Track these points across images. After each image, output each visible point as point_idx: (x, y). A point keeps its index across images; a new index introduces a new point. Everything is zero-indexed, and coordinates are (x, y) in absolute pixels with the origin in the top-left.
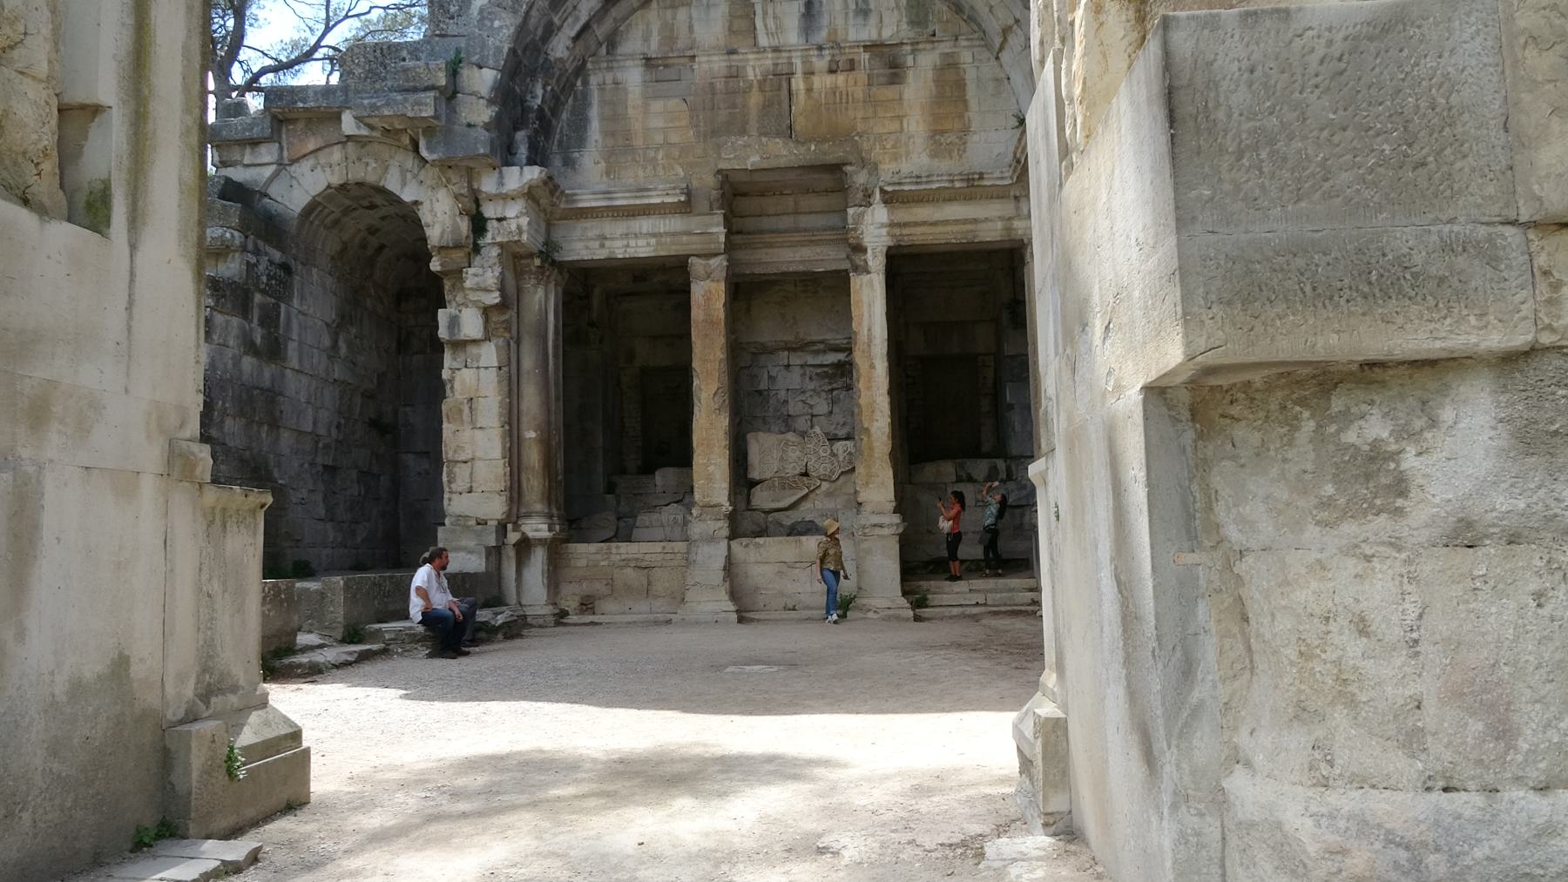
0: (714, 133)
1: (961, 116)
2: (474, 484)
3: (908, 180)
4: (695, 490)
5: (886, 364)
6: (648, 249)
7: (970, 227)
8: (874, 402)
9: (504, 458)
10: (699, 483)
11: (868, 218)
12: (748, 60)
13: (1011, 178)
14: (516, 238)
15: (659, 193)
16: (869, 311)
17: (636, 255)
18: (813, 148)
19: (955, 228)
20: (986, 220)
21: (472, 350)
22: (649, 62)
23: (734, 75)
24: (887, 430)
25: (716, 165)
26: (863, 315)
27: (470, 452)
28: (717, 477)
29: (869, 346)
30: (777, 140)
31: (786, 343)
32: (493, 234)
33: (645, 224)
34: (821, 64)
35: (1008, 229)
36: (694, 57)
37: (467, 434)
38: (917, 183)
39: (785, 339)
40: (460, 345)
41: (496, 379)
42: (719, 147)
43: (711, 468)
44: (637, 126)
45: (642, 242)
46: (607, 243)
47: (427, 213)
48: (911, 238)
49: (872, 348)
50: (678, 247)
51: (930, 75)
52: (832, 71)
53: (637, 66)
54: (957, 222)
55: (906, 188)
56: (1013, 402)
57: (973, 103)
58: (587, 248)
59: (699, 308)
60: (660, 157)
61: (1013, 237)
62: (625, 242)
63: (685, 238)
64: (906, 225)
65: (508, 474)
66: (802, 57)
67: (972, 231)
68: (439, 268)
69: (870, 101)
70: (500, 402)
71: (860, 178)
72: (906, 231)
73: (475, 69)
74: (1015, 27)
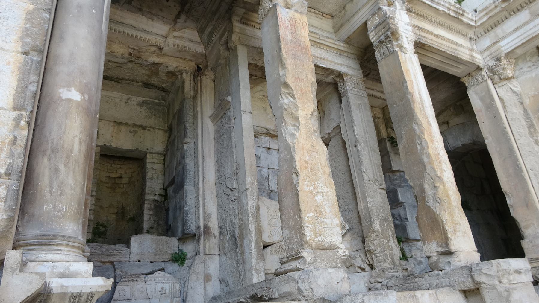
4: (306, 224)
8: (439, 154)
9: (15, 108)
10: (307, 216)
16: (416, 80)
19: (448, 44)
28: (328, 211)
29: (423, 106)
39: (268, 127)
43: (319, 198)
48: (426, 40)
49: (425, 108)
54: (448, 40)
56: (403, 201)
61: (474, 62)
64: (422, 29)
65: (22, 142)
67: (456, 50)
72: (423, 34)
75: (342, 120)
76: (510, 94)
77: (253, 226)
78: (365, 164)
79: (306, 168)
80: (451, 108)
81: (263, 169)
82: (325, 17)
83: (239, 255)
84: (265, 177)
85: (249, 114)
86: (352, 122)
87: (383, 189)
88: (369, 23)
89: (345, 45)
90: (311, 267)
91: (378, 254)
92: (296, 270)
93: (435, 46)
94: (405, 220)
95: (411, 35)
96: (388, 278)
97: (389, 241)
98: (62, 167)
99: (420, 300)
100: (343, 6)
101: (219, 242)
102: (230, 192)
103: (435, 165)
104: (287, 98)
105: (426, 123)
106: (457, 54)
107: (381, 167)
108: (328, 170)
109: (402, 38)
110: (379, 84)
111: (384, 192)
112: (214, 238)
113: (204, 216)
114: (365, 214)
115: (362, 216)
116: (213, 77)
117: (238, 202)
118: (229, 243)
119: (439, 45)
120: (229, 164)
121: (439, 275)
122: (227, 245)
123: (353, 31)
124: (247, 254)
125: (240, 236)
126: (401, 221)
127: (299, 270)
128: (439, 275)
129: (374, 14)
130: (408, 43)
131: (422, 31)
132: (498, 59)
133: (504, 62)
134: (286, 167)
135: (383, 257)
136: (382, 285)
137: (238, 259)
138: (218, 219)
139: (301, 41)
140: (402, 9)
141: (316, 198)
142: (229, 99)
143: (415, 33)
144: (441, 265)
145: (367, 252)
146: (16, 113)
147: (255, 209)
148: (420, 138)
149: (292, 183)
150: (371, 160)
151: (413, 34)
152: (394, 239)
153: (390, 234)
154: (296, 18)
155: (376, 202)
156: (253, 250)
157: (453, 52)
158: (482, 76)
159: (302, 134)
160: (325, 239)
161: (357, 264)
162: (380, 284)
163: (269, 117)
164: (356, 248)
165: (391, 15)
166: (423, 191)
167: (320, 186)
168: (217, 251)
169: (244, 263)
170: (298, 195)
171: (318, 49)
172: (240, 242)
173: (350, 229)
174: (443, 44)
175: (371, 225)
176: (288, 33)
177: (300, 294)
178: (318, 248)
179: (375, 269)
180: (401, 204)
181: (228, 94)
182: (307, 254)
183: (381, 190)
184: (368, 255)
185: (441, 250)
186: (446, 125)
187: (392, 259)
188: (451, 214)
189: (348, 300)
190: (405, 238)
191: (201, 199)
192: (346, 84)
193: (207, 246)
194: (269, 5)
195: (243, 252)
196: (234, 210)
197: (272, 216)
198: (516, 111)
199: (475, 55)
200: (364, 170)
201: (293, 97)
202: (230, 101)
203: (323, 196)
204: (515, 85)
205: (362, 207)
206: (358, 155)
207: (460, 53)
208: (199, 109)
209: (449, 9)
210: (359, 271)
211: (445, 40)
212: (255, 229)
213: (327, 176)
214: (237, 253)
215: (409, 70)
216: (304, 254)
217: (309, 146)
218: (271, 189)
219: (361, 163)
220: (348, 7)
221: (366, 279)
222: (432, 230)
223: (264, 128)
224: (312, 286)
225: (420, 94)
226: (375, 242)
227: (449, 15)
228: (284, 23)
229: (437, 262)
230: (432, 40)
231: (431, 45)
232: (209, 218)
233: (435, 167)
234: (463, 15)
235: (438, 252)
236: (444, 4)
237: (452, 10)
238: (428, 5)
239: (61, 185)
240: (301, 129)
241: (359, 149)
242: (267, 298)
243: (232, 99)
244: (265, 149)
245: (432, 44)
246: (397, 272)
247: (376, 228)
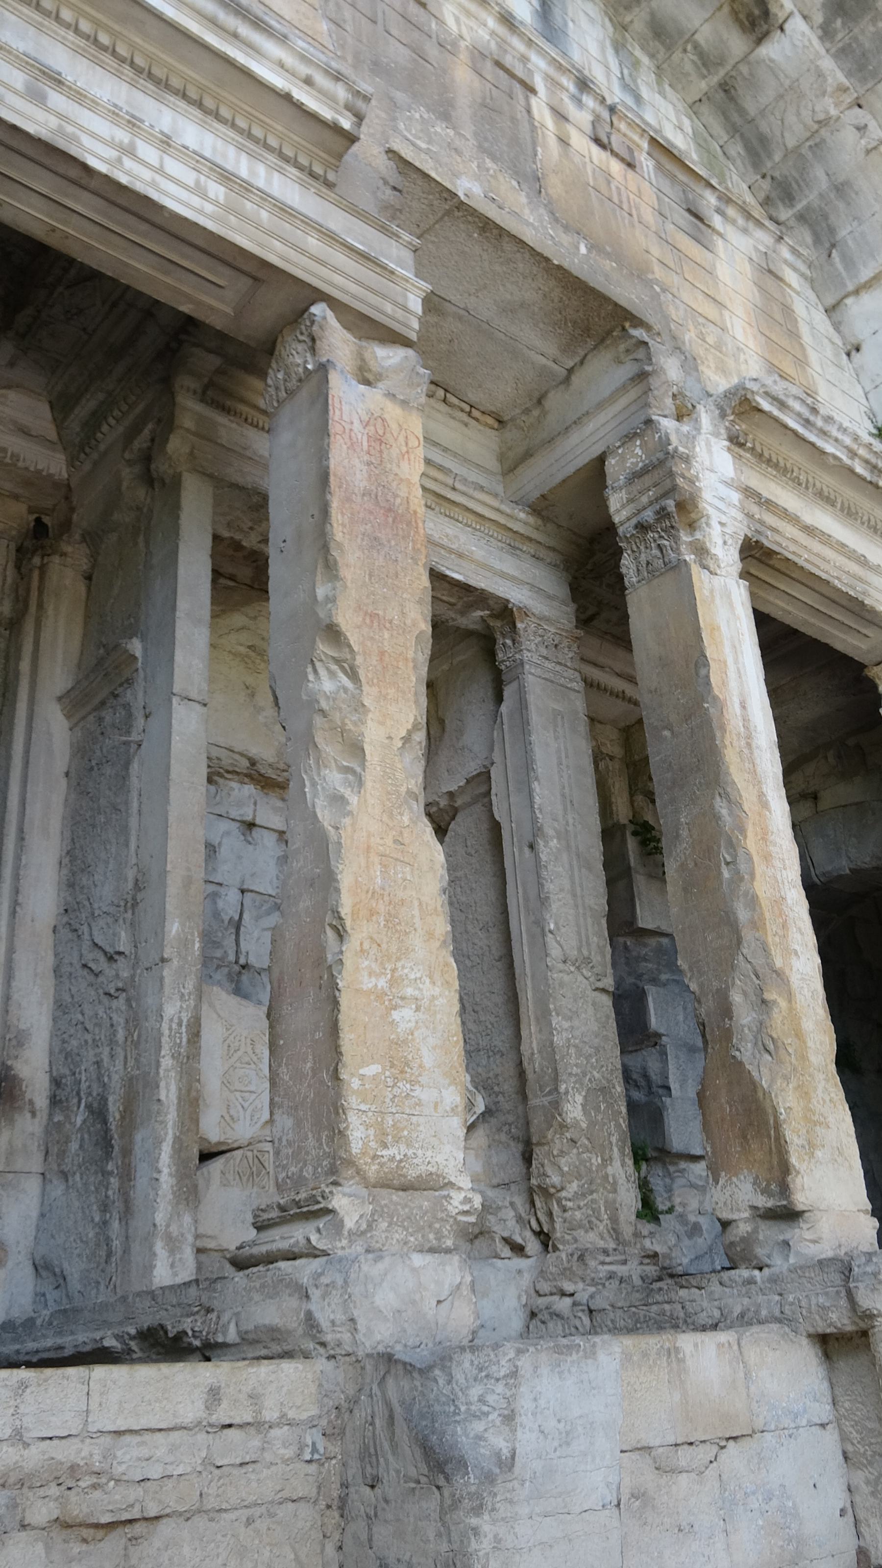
4: (352, 1102)
7: (854, 568)
16: (736, 661)
17: (154, 195)
18: (583, 250)
19: (841, 560)
26: (725, 662)
28: (428, 1058)
29: (749, 745)
31: (253, 763)
38: (807, 423)
39: (254, 751)
43: (404, 1016)
46: (56, 99)
48: (778, 538)
49: (756, 753)
52: (597, 141)
54: (841, 548)
56: (662, 1031)
59: (352, 446)
62: (122, 136)
63: (313, 243)
64: (768, 504)
67: (860, 580)
72: (771, 520)
75: (497, 756)
77: (173, 1088)
78: (554, 907)
79: (372, 913)
80: (831, 754)
81: (222, 891)
82: (477, 420)
83: (114, 1181)
84: (226, 918)
85: (198, 707)
86: (528, 765)
87: (603, 990)
88: (611, 462)
89: (531, 520)
90: (358, 1248)
91: (570, 1200)
92: (307, 1255)
93: (801, 562)
94: (661, 1091)
95: (735, 519)
96: (594, 1282)
97: (607, 1161)
99: (689, 1362)
100: (536, 395)
101: (47, 1132)
102: (102, 964)
103: (769, 933)
104: (332, 674)
105: (755, 799)
106: (864, 593)
107: (604, 922)
108: (442, 926)
109: (708, 524)
110: (621, 653)
111: (606, 1001)
112: (28, 1115)
114: (542, 1070)
115: (530, 1075)
116: (84, 564)
117: (128, 1000)
118: (82, 1139)
119: (813, 558)
120: (111, 867)
121: (751, 1281)
122: (74, 1146)
123: (560, 477)
124: (141, 1182)
125: (123, 1118)
126: (650, 1093)
127: (314, 1253)
128: (751, 1281)
129: (629, 437)
130: (725, 543)
131: (768, 509)
134: (305, 903)
135: (584, 1210)
136: (575, 1304)
137: (107, 1197)
138: (51, 1053)
139: (396, 496)
140: (716, 435)
141: (396, 1015)
142: (136, 647)
143: (747, 515)
144: (761, 1252)
147: (184, 1029)
148: (732, 846)
149: (320, 961)
150: (574, 895)
151: (740, 516)
152: (622, 1153)
153: (614, 1139)
154: (386, 416)
155: (577, 1033)
156: (166, 1171)
157: (851, 586)
159: (371, 801)
160: (410, 1153)
161: (500, 1231)
162: (568, 1301)
163: (261, 719)
164: (502, 1177)
165: (681, 449)
166: (726, 1011)
167: (412, 976)
168: (36, 1163)
169: (127, 1212)
170: (335, 1003)
171: (447, 519)
172: (122, 1137)
173: (488, 1113)
174: (824, 559)
175: (556, 1105)
176: (356, 462)
177: (313, 1337)
178: (385, 1184)
179: (556, 1249)
180: (653, 1039)
181: (132, 631)
183: (597, 994)
184: (538, 1204)
185: (763, 1202)
186: (809, 804)
187: (614, 1219)
188: (805, 1093)
189: (467, 1364)
190: (657, 1149)
192: (520, 643)
194: (306, 362)
195: (127, 1175)
196: (112, 1025)
197: (240, 1053)
200: (552, 926)
201: (353, 675)
202: (138, 653)
203: (418, 1009)
205: (535, 1045)
206: (539, 876)
207: (872, 592)
208: (25, 666)
209: (853, 454)
210: (506, 1252)
211: (832, 547)
212: (179, 1098)
213: (438, 944)
214: (106, 1174)
215: (719, 628)
216: (340, 1202)
217: (389, 841)
218: (242, 961)
219: (543, 901)
220: (554, 400)
221: (526, 1280)
222: (745, 1137)
223: (242, 754)
224: (356, 1313)
225: (743, 707)
226: (565, 1163)
227: (852, 471)
228: (347, 427)
229: (748, 1241)
230: (795, 541)
231: (790, 556)
232: (20, 1044)
233: (770, 939)
235: (754, 1208)
236: (840, 436)
237: (861, 458)
238: (795, 433)
240: (369, 784)
241: (544, 857)
242: (197, 1343)
243: (145, 650)
244: (238, 824)
245: (794, 553)
246: (624, 1262)
247: (572, 1116)
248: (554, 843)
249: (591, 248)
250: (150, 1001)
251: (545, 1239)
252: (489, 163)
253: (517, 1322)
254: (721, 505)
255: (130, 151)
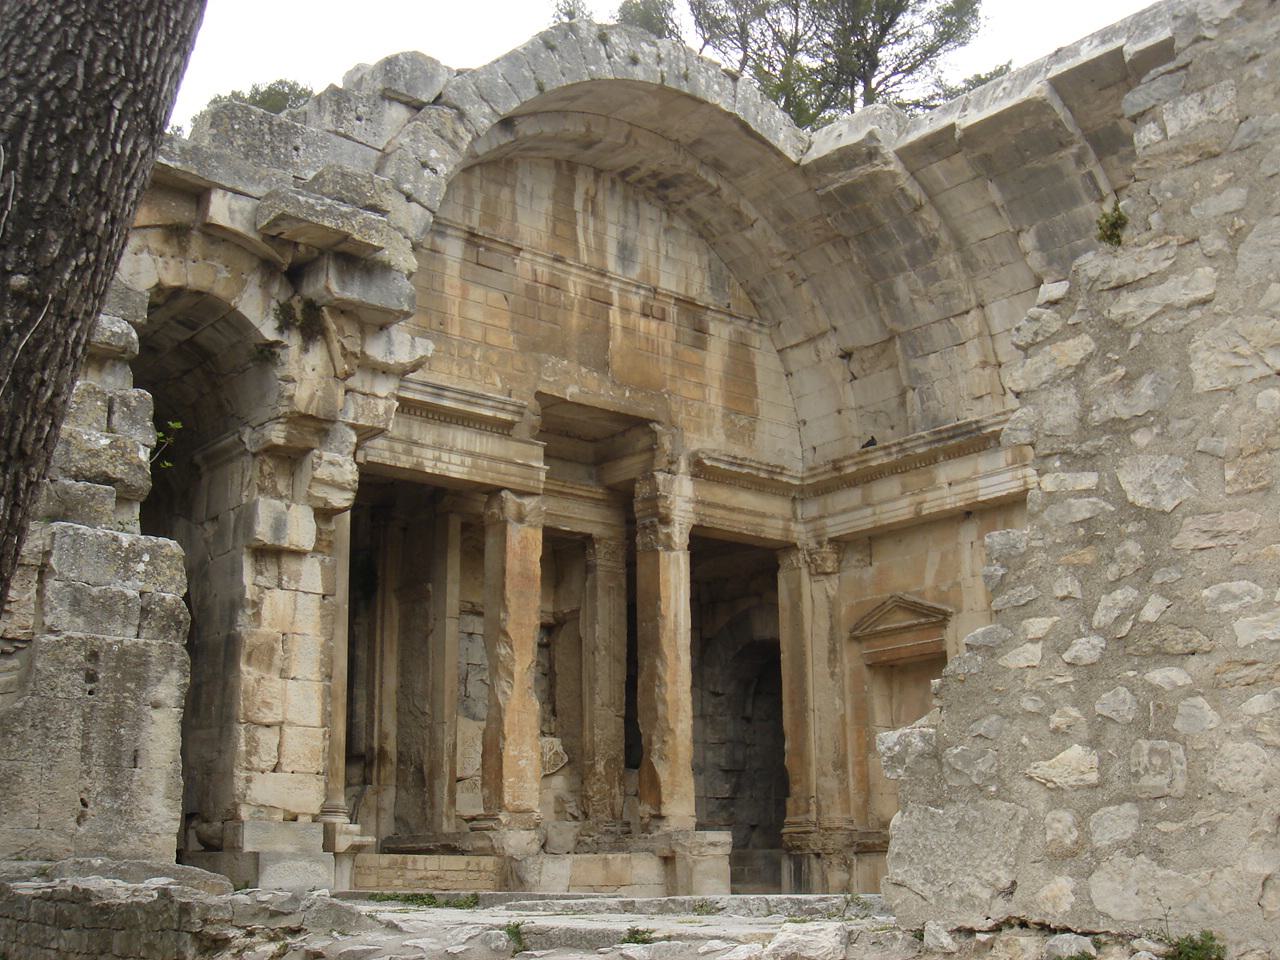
0: (535, 347)
1: (751, 402)
2: (282, 760)
3: (726, 459)
5: (689, 657)
6: (461, 469)
7: (758, 520)
8: (679, 699)
10: (509, 780)
11: (676, 485)
12: (569, 273)
13: (802, 479)
14: (382, 426)
15: (496, 404)
18: (627, 394)
19: (748, 518)
20: (773, 516)
21: (290, 565)
22: (472, 238)
23: (554, 286)
24: (689, 733)
25: (535, 386)
27: (280, 711)
28: (529, 774)
29: (675, 634)
30: (595, 374)
32: (356, 413)
33: (461, 437)
34: (636, 301)
35: (787, 530)
36: (520, 249)
37: (274, 684)
38: (731, 464)
39: (473, 600)
40: (270, 554)
41: (318, 613)
42: (539, 364)
43: (523, 763)
44: (454, 310)
45: (456, 459)
46: (416, 450)
47: (293, 362)
50: (495, 475)
51: (727, 349)
52: (645, 315)
53: (457, 237)
55: (722, 466)
57: (760, 388)
58: (392, 450)
60: (477, 356)
62: (437, 453)
64: (711, 505)
66: (621, 289)
68: (281, 442)
69: (676, 358)
70: (323, 645)
71: (666, 443)
72: (709, 511)
73: (404, 198)
74: (829, 334)
76: (824, 597)
78: (600, 682)
88: (637, 485)
98: (336, 756)
102: (419, 714)
111: (621, 720)
113: (380, 737)
122: (410, 779)
129: (645, 478)
132: (820, 544)
133: (827, 548)
142: (430, 586)
145: (584, 799)
146: (323, 730)
148: (660, 678)
149: (498, 746)
151: (692, 515)
158: (798, 560)
168: (393, 781)
169: (433, 806)
173: (569, 762)
175: (593, 765)
182: (503, 817)
185: (654, 812)
187: (612, 810)
191: (376, 711)
193: (382, 774)
195: (432, 794)
198: (824, 624)
199: (793, 526)
201: (511, 647)
204: (831, 585)
209: (758, 469)
219: (596, 680)
221: (577, 830)
225: (676, 616)
234: (781, 473)
239: (337, 769)
240: (515, 687)
248: (603, 653)
249: (635, 390)
250: (439, 736)
251: (586, 815)
252: (584, 370)
253: (571, 845)
254: (682, 514)
255: (438, 459)
